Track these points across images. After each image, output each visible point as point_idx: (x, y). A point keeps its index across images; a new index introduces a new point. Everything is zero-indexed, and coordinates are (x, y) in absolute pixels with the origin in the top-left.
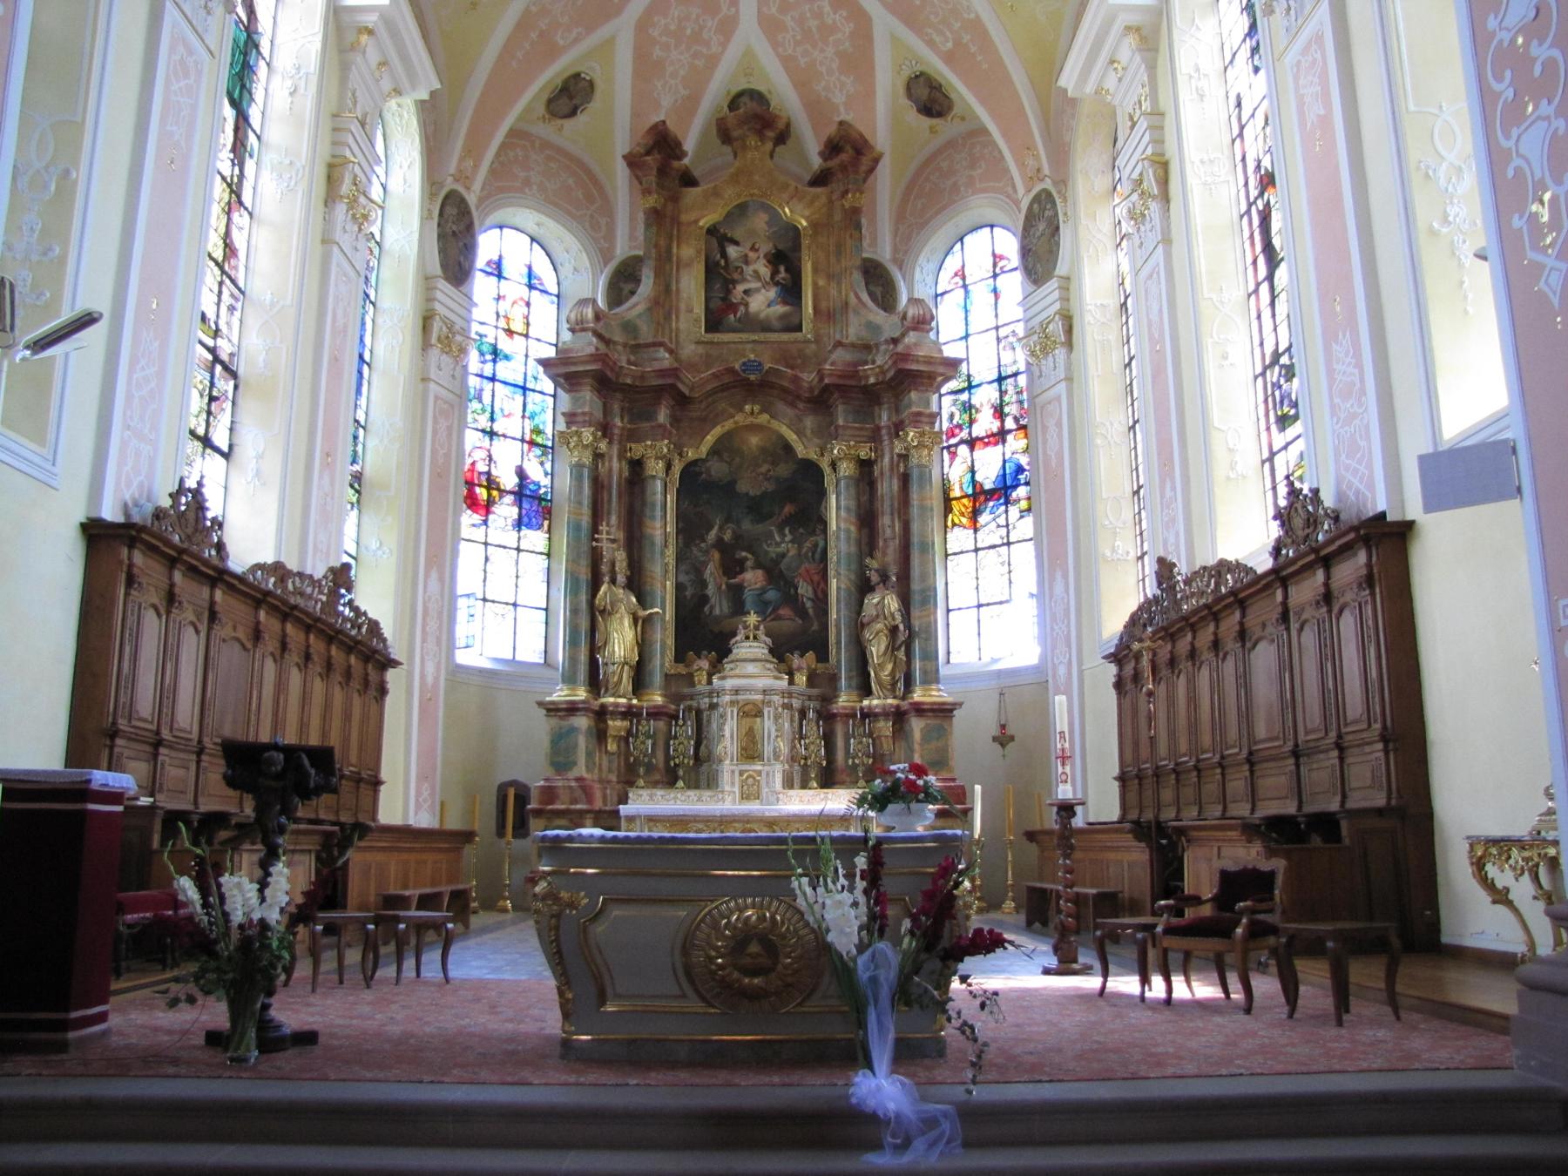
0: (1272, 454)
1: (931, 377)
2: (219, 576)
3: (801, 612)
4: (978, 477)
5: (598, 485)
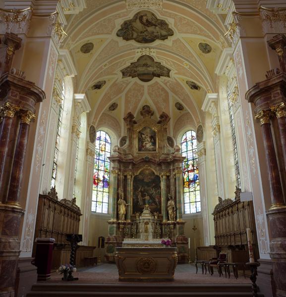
0: (238, 179)
1: (180, 160)
2: (56, 202)
3: (156, 204)
4: (190, 178)
5: (118, 180)
